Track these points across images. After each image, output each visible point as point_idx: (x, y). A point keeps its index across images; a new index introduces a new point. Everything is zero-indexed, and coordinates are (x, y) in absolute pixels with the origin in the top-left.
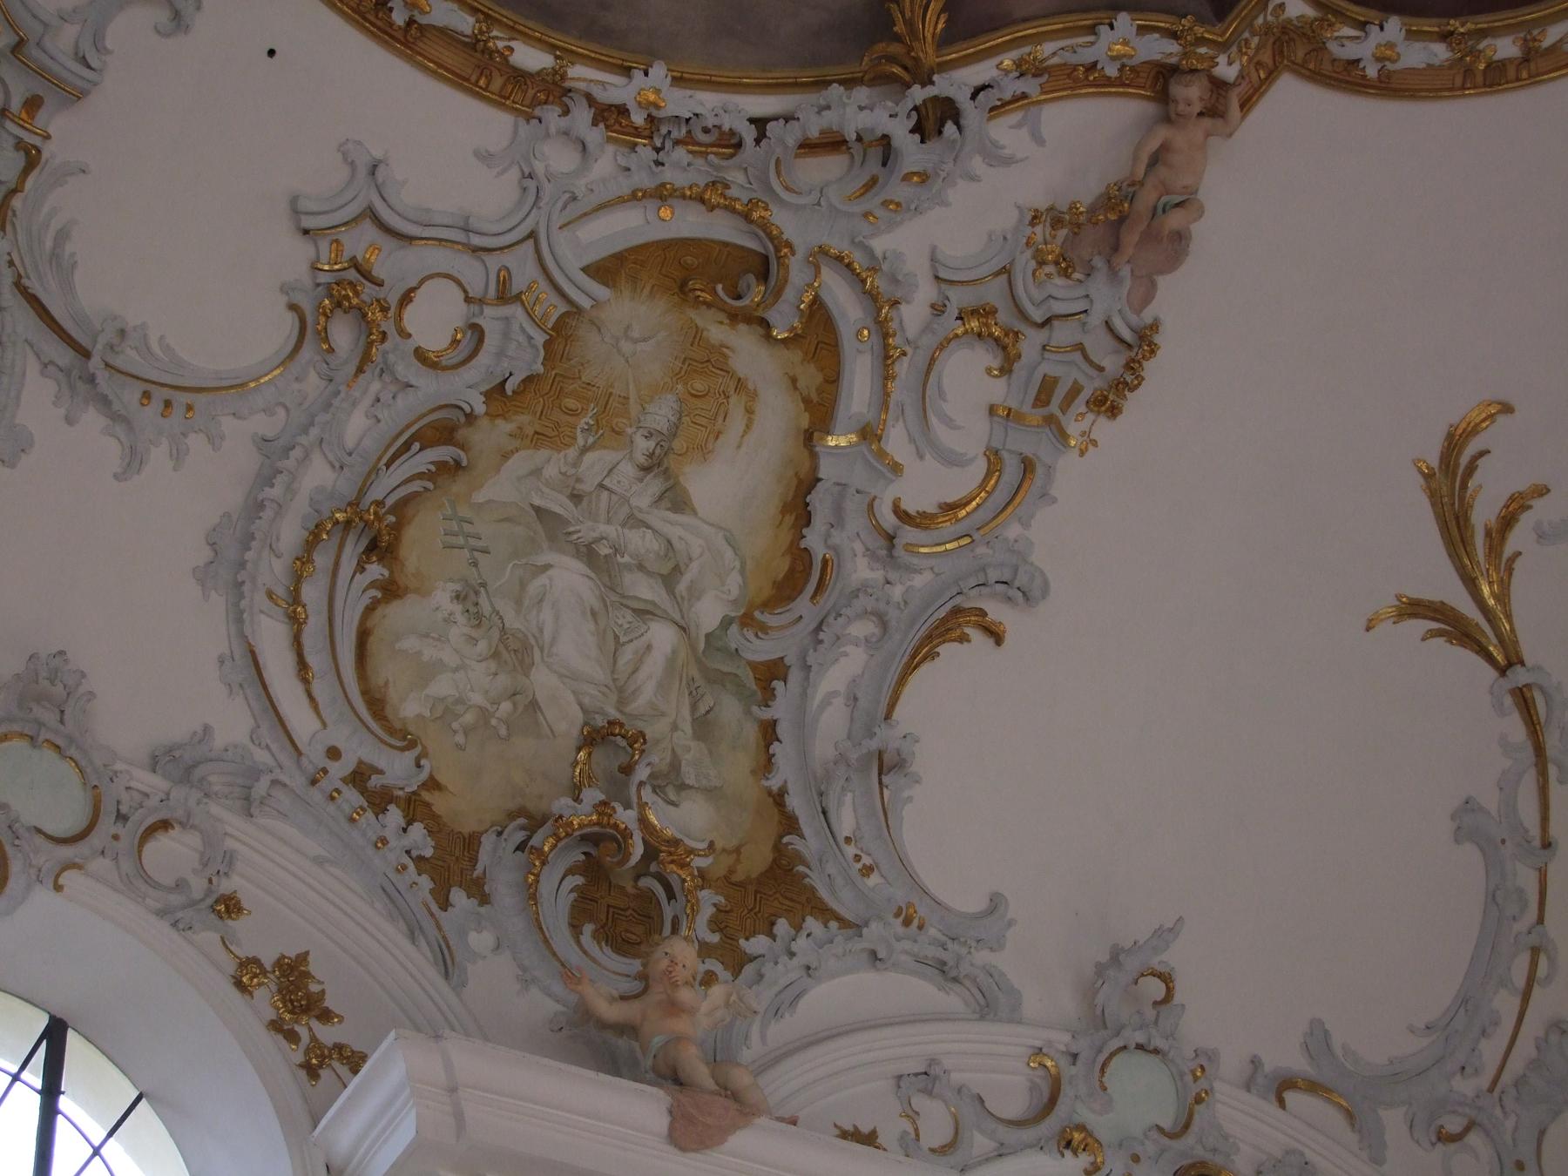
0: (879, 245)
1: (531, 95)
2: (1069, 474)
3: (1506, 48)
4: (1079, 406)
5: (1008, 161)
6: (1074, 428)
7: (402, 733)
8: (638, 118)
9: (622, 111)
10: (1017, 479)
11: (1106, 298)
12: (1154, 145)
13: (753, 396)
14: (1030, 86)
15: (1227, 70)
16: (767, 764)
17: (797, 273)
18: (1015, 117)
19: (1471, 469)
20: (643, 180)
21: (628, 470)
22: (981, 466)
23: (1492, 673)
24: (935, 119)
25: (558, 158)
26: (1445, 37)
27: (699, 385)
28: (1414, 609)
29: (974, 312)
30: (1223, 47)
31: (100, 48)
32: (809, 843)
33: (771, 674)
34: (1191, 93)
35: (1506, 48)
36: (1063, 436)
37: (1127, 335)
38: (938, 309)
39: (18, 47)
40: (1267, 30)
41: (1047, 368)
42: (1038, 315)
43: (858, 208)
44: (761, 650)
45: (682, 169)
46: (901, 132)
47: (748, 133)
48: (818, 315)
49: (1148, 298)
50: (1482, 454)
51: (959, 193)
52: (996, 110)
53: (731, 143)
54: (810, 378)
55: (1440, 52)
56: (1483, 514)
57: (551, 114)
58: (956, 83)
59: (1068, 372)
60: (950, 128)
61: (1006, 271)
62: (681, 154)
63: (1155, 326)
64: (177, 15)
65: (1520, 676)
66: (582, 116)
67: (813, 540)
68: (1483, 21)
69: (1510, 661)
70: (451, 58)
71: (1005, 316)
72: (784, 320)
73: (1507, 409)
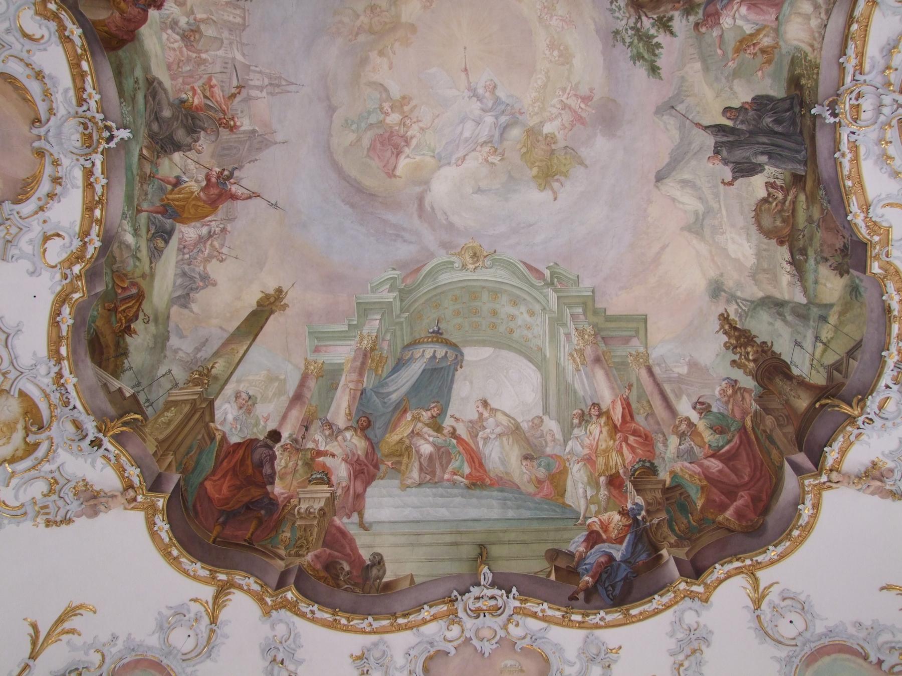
0: (60, 450)
1: (55, 354)
2: (27, 525)
3: (175, 553)
4: (45, 517)
5: (94, 467)
6: (38, 520)
8: (62, 381)
9: (62, 377)
11: (74, 506)
12: (116, 493)
13: (8, 443)
14: (113, 459)
15: (140, 498)
17: (43, 436)
18: (104, 462)
19: (75, 615)
20: (48, 391)
22: (17, 504)
23: (28, 656)
24: (96, 443)
25: (43, 370)
26: (170, 539)
27: (5, 429)
28: (34, 626)
29: (55, 480)
30: (144, 495)
31: (17, 260)
34: (131, 493)
35: (175, 553)
36: (37, 516)
37: (68, 517)
38: (51, 472)
39: (9, 241)
40: (152, 501)
41: (51, 505)
42: (62, 495)
43: (66, 440)
45: (55, 398)
46: (91, 437)
47: (71, 407)
48: (37, 445)
49: (79, 516)
50: (81, 615)
51: (81, 460)
52: (104, 456)
53: (66, 404)
54: (20, 453)
55: (167, 540)
56: (67, 625)
57: (53, 362)
58: (107, 444)
59: (52, 509)
60: (96, 448)
61: (69, 481)
62: (59, 395)
63: (73, 521)
64: (33, 273)
65: (31, 662)
66: (56, 369)
68: (177, 544)
69: (33, 656)
70: (54, 335)
71: (57, 487)
72: (31, 439)
73: (95, 612)
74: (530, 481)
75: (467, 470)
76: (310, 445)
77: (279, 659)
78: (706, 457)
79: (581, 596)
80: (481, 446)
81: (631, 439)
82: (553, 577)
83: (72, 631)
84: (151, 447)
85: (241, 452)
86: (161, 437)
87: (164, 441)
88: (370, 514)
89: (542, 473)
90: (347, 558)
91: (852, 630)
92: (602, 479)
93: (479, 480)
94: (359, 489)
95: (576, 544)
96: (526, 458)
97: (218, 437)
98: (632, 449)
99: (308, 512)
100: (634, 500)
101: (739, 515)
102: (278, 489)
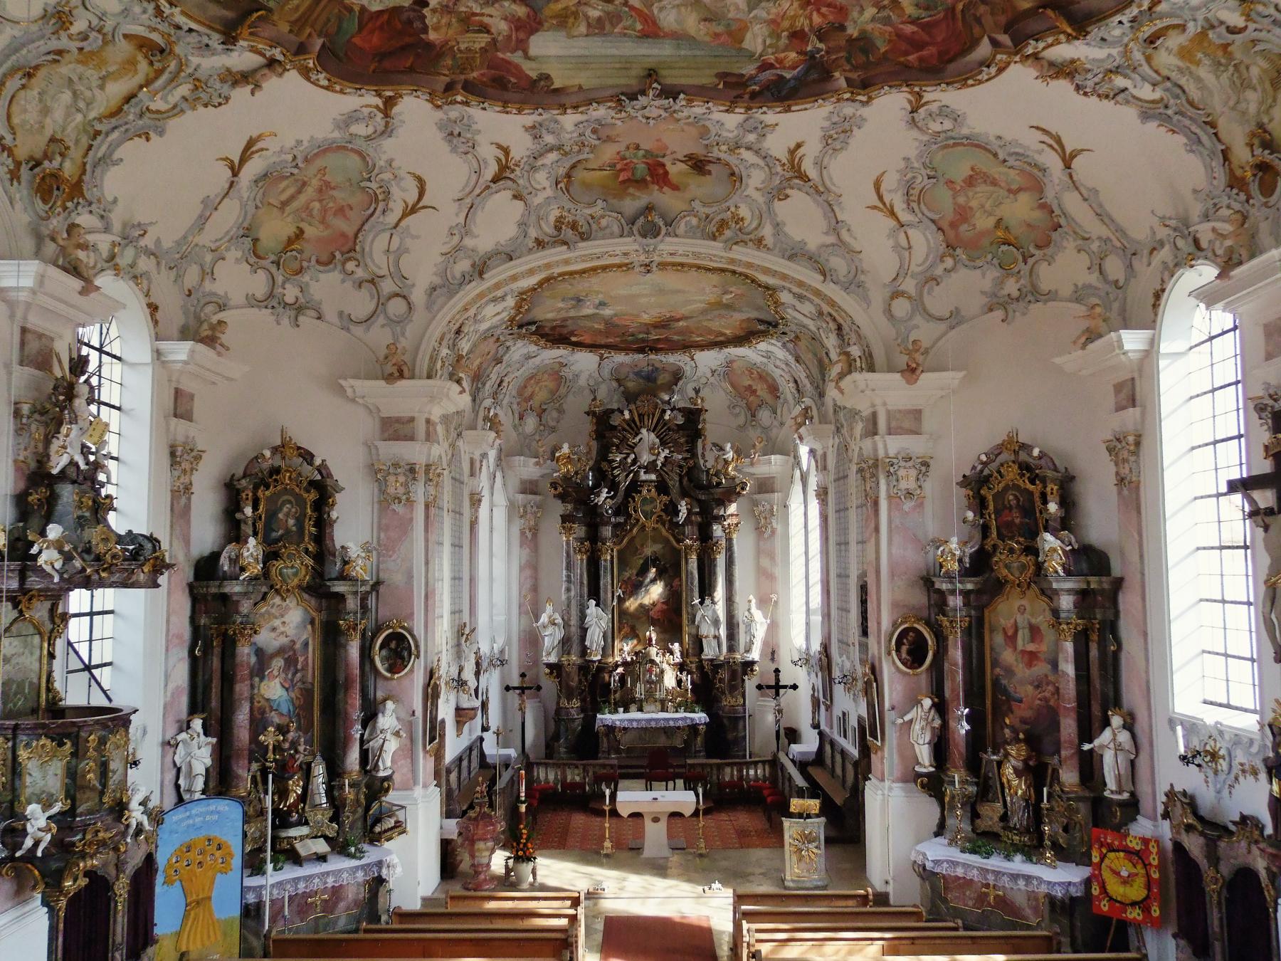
3: (338, 88)
7: (12, 128)
10: (176, 111)
16: (86, 155)
21: (96, 77)
32: (86, 178)
33: (98, 133)
44: (98, 127)
67: (125, 107)
74: (707, 34)
75: (639, 26)
76: (463, 9)
77: (456, 133)
78: (903, 23)
79: (747, 96)
80: (656, 12)
81: (824, 10)
82: (721, 86)
83: (262, 150)
84: (285, 28)
85: (386, 16)
86: (293, 19)
87: (297, 20)
88: (533, 51)
89: (720, 29)
90: (513, 75)
91: (992, 138)
92: (785, 34)
93: (651, 31)
94: (522, 35)
95: (749, 69)
96: (705, 20)
97: (357, 9)
98: (823, 16)
99: (469, 50)
100: (814, 44)
101: (921, 59)
102: (432, 36)
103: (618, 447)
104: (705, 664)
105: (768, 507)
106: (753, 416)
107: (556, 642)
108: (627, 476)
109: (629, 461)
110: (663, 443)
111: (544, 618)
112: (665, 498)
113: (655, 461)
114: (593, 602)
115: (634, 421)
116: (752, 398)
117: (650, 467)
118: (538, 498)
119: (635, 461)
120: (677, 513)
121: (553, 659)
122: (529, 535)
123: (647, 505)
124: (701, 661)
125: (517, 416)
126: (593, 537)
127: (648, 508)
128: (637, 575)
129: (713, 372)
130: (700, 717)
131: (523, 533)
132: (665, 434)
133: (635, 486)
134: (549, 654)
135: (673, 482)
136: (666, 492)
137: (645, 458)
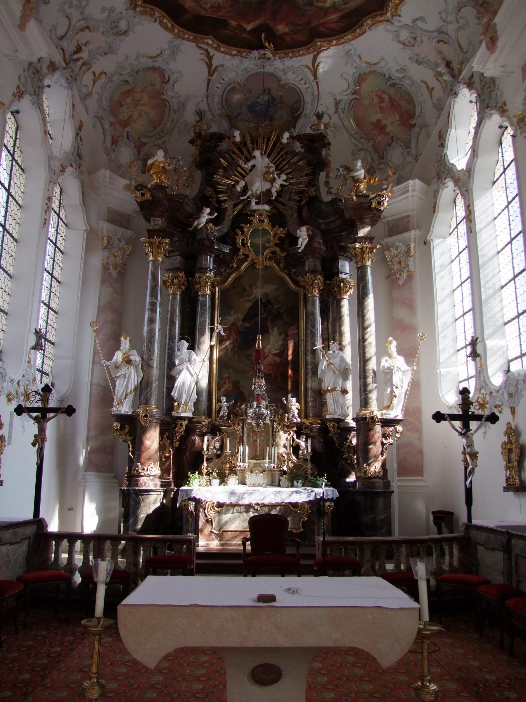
103: (225, 169)
104: (330, 425)
105: (403, 248)
106: (381, 157)
107: (131, 387)
108: (235, 205)
109: (239, 189)
110: (280, 169)
111: (118, 356)
112: (281, 232)
113: (269, 191)
114: (186, 344)
115: (245, 144)
116: (380, 138)
117: (265, 197)
118: (129, 233)
119: (245, 189)
120: (295, 240)
121: (126, 409)
122: (114, 274)
123: (257, 238)
124: (324, 422)
125: (109, 138)
126: (190, 267)
127: (260, 241)
128: (244, 320)
129: (337, 104)
130: (323, 490)
131: (105, 268)
132: (280, 157)
133: (244, 217)
134: (121, 403)
135: (290, 213)
136: (283, 224)
137: (258, 186)
